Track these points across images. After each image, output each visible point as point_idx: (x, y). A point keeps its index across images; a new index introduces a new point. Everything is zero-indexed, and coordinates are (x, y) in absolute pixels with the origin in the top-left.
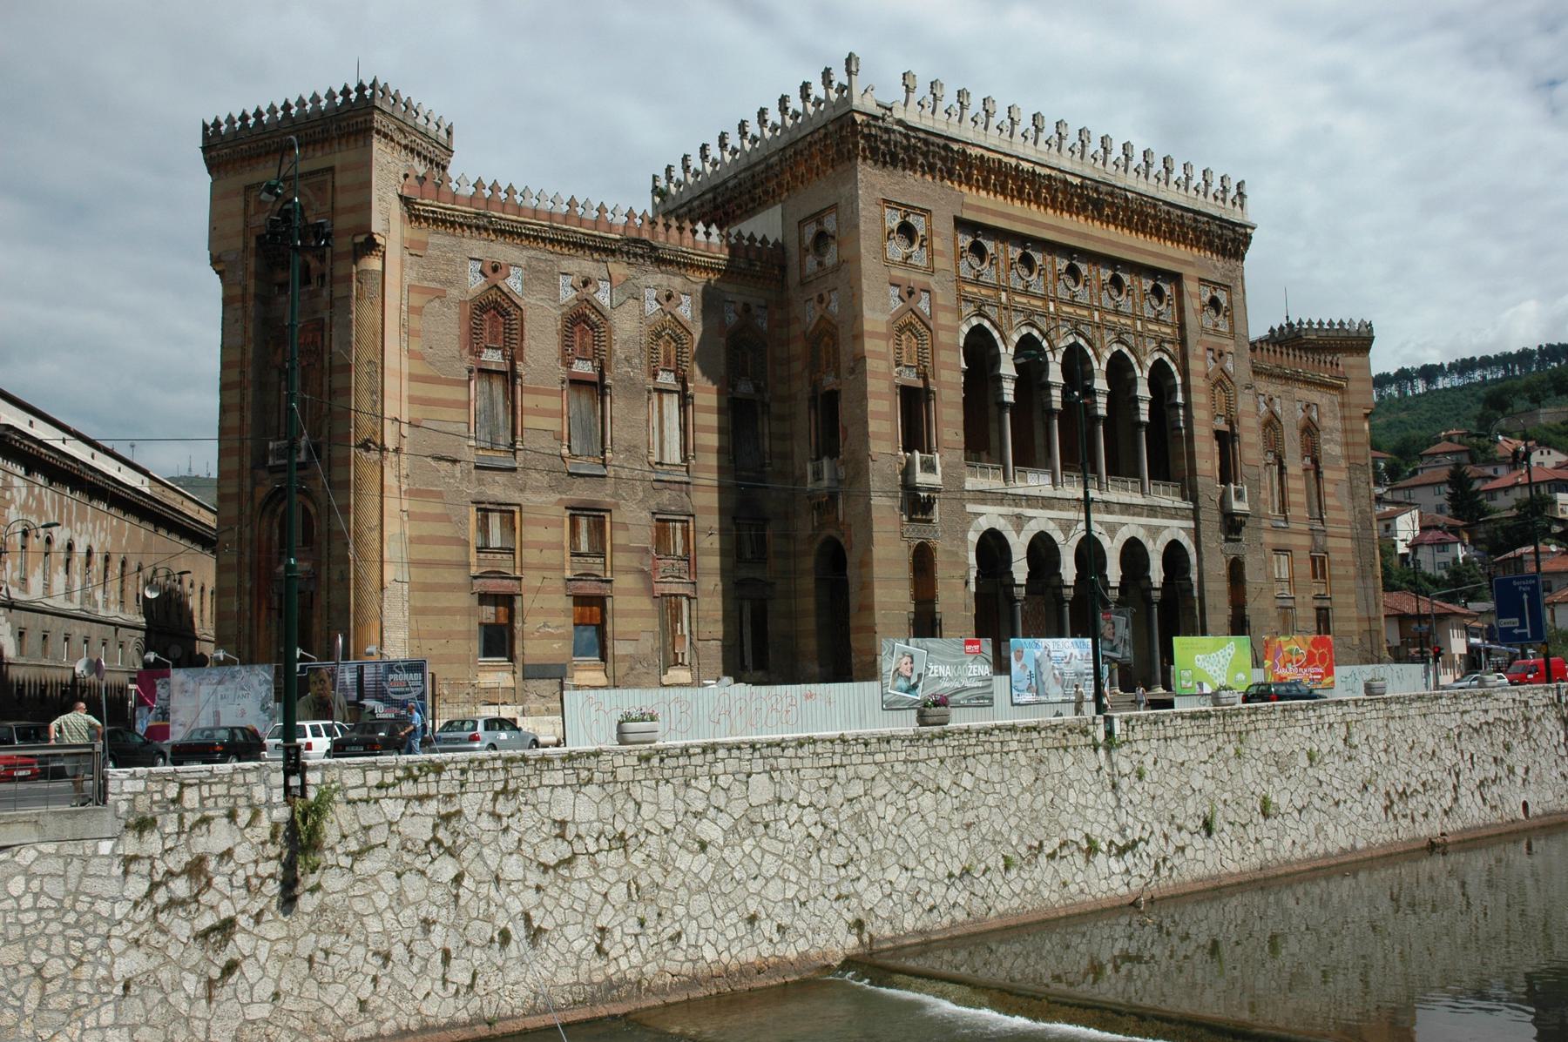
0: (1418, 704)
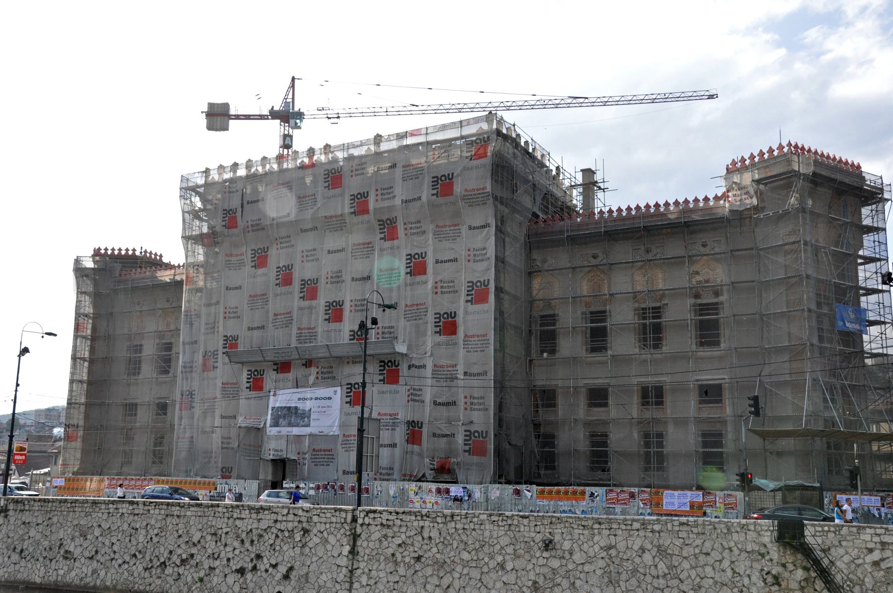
0: (195, 509)
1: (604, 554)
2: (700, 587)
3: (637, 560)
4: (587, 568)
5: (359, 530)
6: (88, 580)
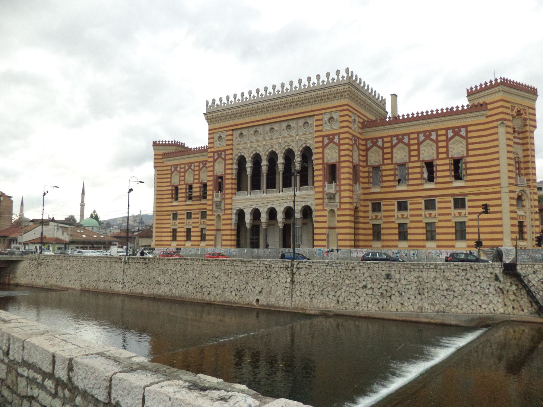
1: (416, 280)
2: (464, 295)
3: (432, 283)
4: (407, 287)
5: (295, 270)
6: (168, 293)
